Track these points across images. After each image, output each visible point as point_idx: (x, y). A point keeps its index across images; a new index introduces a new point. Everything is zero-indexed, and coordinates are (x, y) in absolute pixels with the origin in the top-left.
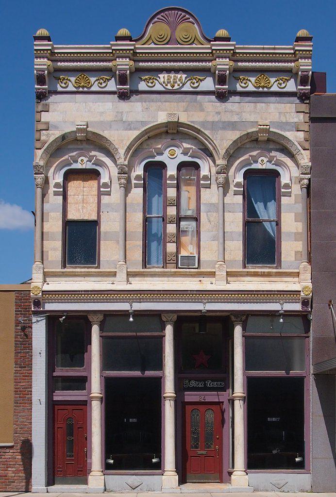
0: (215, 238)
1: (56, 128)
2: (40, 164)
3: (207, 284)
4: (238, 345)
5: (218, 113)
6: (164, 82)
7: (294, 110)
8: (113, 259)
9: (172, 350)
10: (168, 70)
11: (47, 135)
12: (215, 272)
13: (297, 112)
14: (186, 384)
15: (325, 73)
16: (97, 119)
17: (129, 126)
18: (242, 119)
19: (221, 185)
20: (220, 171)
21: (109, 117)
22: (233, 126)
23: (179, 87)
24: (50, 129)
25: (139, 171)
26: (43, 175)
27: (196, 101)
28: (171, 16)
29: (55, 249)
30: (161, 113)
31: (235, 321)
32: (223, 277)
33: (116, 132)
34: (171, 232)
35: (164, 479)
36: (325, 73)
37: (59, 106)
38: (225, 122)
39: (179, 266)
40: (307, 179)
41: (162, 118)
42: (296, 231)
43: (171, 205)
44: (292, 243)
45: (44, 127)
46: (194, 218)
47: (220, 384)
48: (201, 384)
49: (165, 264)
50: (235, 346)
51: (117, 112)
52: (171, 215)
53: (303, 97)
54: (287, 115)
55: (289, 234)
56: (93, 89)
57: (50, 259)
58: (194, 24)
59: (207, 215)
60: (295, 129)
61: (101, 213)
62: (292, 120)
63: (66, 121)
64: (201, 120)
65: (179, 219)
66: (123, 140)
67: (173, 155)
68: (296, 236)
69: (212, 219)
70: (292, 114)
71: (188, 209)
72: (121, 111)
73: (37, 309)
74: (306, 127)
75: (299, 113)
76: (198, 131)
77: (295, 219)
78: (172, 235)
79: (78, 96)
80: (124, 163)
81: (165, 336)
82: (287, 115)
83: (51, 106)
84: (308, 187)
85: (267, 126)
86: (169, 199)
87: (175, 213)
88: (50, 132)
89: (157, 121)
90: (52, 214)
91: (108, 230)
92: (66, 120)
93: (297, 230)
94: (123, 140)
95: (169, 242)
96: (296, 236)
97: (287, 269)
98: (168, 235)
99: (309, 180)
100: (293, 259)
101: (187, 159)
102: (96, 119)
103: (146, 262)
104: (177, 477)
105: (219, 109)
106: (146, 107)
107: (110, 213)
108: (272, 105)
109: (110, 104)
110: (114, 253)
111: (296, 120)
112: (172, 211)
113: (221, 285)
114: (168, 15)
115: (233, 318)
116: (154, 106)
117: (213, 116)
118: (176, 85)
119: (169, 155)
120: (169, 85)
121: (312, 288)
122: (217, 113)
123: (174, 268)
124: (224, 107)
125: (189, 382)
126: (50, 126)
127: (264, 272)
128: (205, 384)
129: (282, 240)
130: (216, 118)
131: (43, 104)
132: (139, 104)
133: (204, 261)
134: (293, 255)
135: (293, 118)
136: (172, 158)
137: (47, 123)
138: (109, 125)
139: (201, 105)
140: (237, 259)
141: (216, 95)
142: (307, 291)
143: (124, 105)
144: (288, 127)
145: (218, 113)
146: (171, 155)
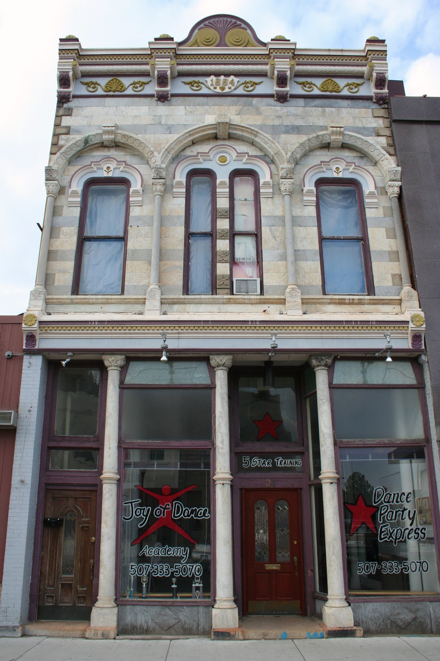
0: (284, 257)
1: (78, 132)
2: (53, 168)
3: (274, 313)
4: (324, 401)
5: (280, 117)
6: (212, 85)
7: (371, 115)
8: (142, 284)
9: (227, 389)
10: (217, 74)
11: (67, 140)
12: (285, 299)
13: (375, 117)
14: (246, 463)
15: (402, 82)
16: (129, 122)
17: (170, 129)
18: (309, 123)
19: (288, 193)
20: (285, 175)
21: (146, 120)
22: (296, 130)
23: (230, 90)
24: (71, 133)
25: (181, 177)
26: (56, 182)
27: (251, 105)
28: (222, 23)
29: (64, 272)
30: (209, 116)
31: (318, 366)
32: (297, 305)
33: (153, 136)
34: (222, 250)
35: (216, 615)
36: (402, 82)
37: (84, 111)
38: (287, 126)
39: (235, 292)
40: (397, 187)
41: (210, 119)
42: (390, 250)
43: (223, 237)
44: (387, 263)
45: (64, 131)
46: (254, 234)
47: (296, 462)
48: (268, 463)
49: (214, 289)
50: (319, 402)
51: (154, 116)
52: (223, 230)
53: (381, 101)
54: (364, 120)
55: (381, 253)
56: (127, 92)
57: (56, 284)
58: (246, 30)
59: (271, 229)
60: (374, 134)
61: (129, 228)
62: (369, 126)
63: (91, 126)
64: (259, 123)
65: (233, 235)
66: (161, 144)
67: (224, 162)
68: (393, 256)
69: (277, 234)
70: (370, 119)
71: (244, 220)
72: (159, 114)
73: (29, 347)
74: (387, 132)
75: (377, 119)
76: (256, 134)
77: (387, 235)
78: (224, 253)
79: (108, 99)
80: (160, 166)
81: (215, 388)
82: (364, 120)
83: (74, 111)
84: (400, 197)
85: (341, 127)
86: (220, 211)
87: (227, 227)
88: (71, 137)
89: (204, 123)
90: (65, 229)
91: (138, 248)
92: (92, 124)
93: (390, 247)
94: (161, 144)
95: (221, 262)
96: (393, 256)
97: (383, 295)
98: (218, 254)
99: (401, 188)
100: (390, 284)
101: (240, 166)
102: (129, 123)
103: (186, 290)
104: (237, 610)
105: (280, 113)
106: (190, 110)
107: (140, 228)
108: (344, 110)
109: (147, 108)
110: (144, 275)
111: (374, 125)
112: (223, 224)
113: (295, 314)
114: (216, 22)
115: (314, 362)
116: (200, 109)
117: (273, 120)
118: (227, 87)
119: (218, 162)
120: (218, 87)
121: (425, 316)
122: (277, 116)
123: (227, 294)
124: (286, 111)
125: (251, 460)
126: (71, 130)
127: (353, 299)
128: (274, 463)
129: (372, 260)
130: (277, 122)
131: (65, 108)
132: (182, 108)
133: (270, 286)
134: (390, 279)
135: (371, 123)
136: (222, 162)
137: (68, 128)
138: (144, 129)
139: (257, 109)
140: (314, 284)
141: (276, 99)
142: (418, 321)
143: (162, 109)
144: (366, 132)
145: (280, 117)
146: (221, 162)
